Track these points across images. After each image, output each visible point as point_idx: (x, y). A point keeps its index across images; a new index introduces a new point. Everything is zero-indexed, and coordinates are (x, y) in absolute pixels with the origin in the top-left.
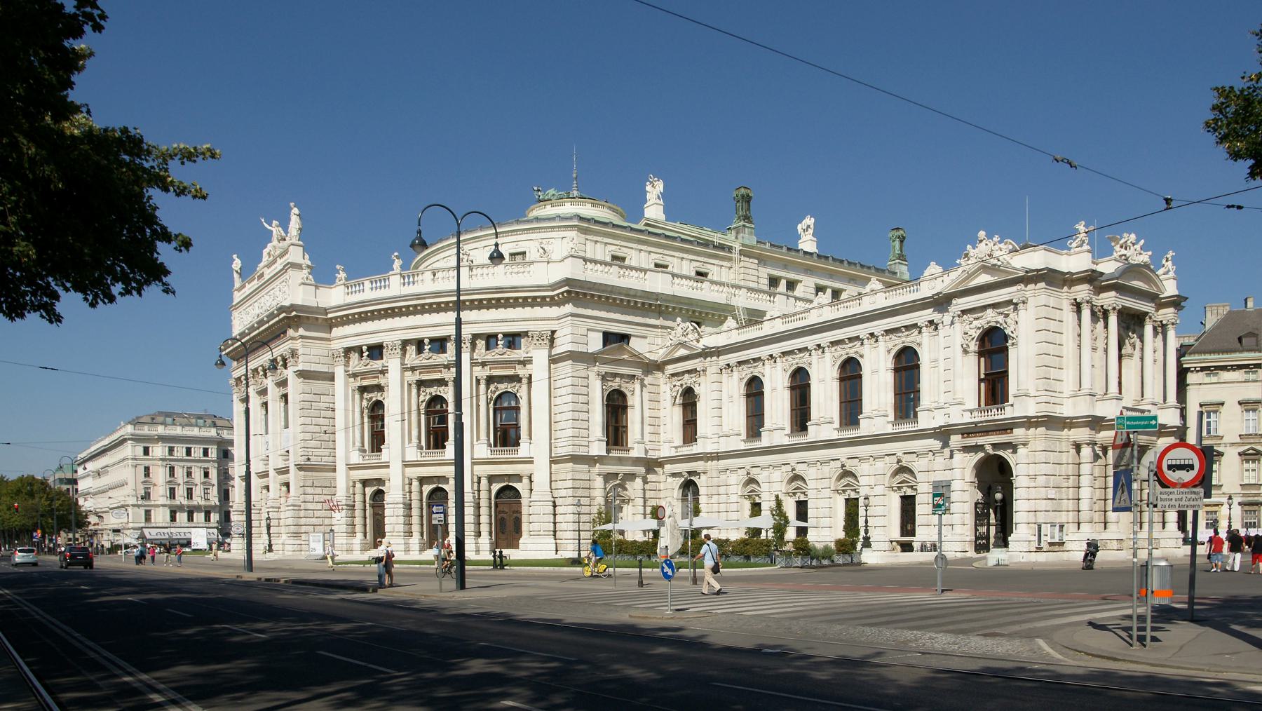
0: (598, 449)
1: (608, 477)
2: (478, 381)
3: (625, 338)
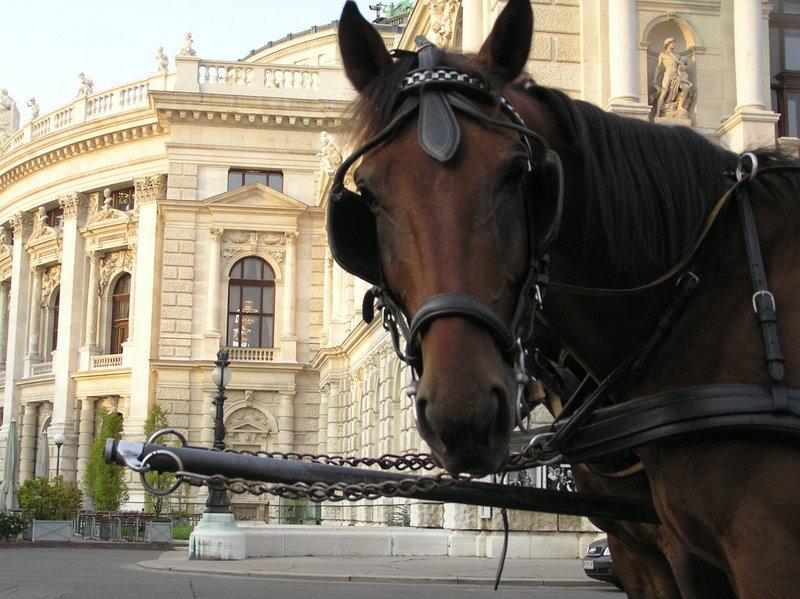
3: (280, 173)
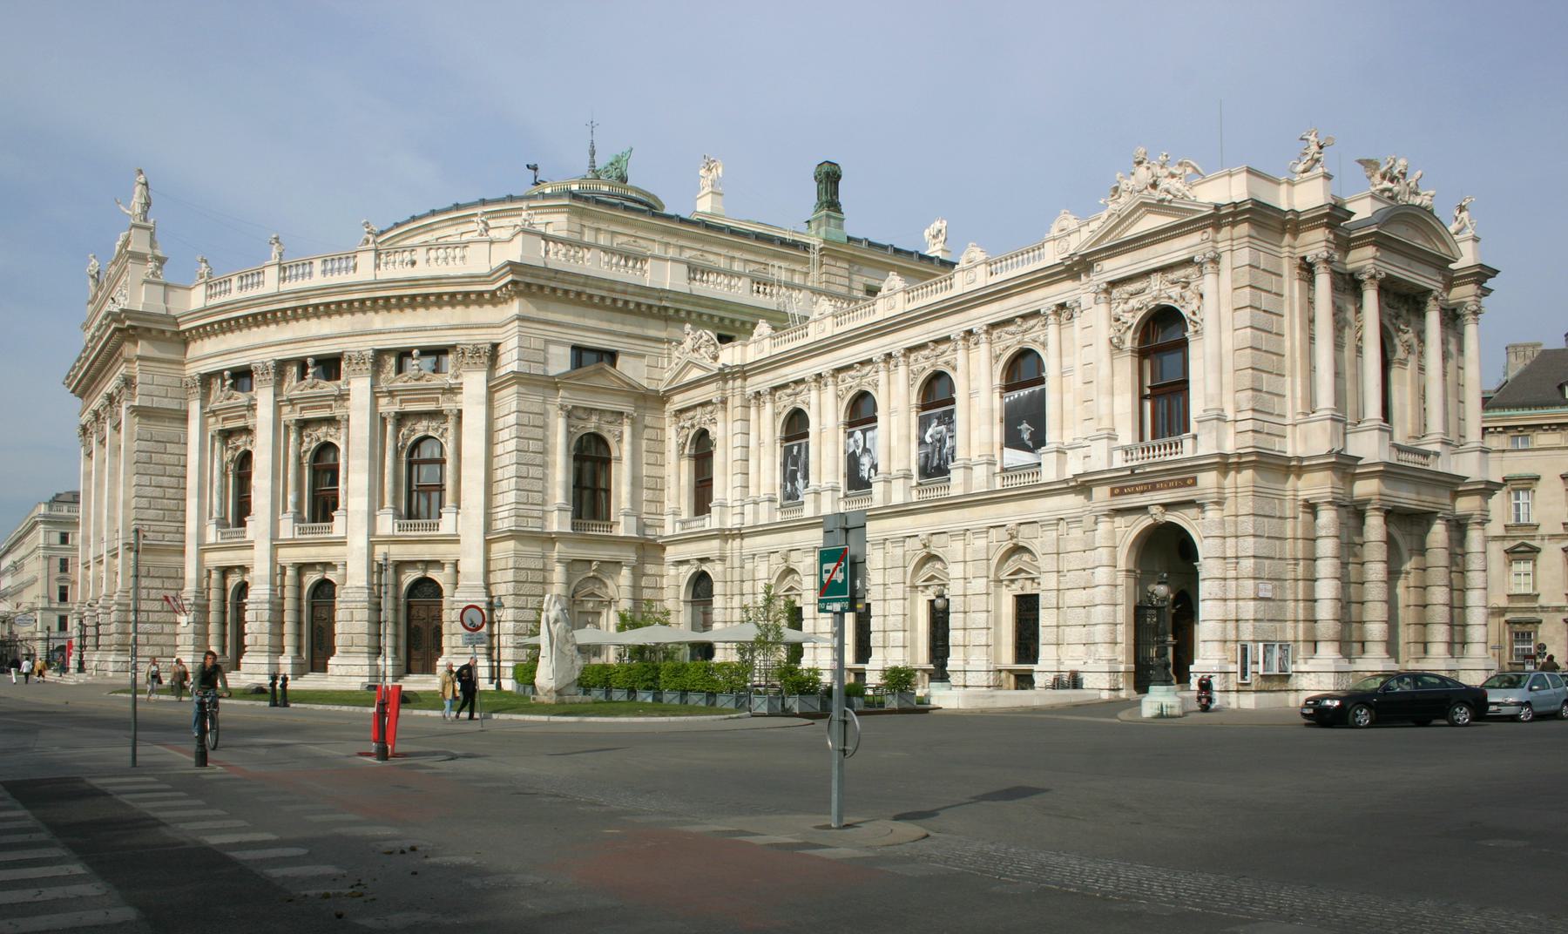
0: (559, 522)
1: (571, 565)
3: (612, 356)
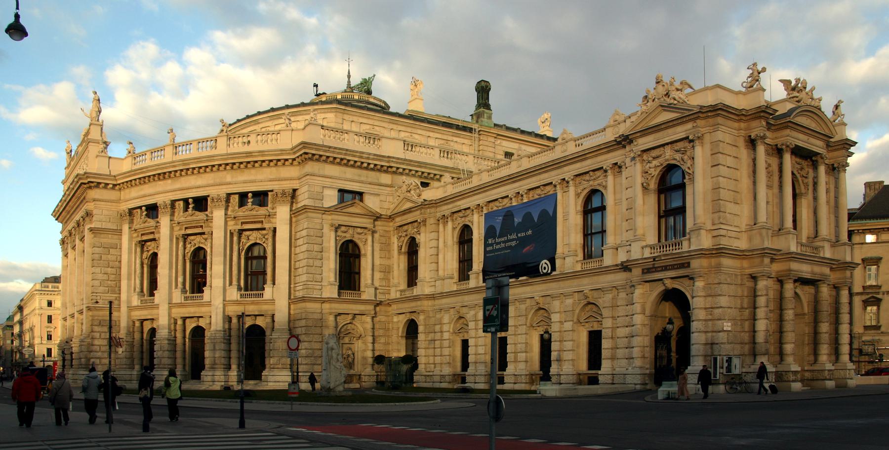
2: (232, 234)
3: (361, 194)
